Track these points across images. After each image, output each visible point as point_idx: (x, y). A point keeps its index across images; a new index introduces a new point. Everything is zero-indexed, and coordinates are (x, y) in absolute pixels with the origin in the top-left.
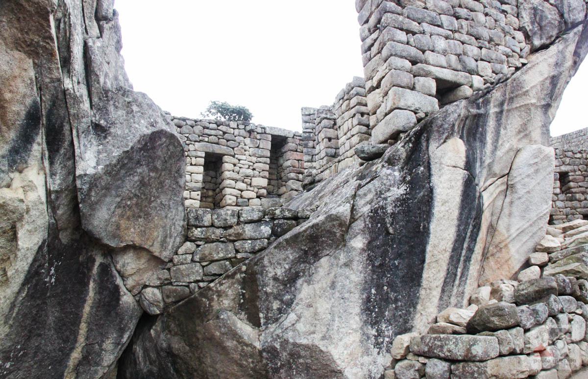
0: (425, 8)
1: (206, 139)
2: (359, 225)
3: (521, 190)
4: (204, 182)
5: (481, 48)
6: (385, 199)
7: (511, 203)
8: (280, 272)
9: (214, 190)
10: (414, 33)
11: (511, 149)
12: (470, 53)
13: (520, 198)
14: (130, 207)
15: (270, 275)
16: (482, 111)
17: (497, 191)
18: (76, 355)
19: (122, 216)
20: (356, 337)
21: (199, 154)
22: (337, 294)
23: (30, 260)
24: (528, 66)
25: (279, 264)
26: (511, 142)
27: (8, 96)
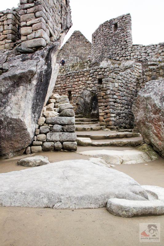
6: (43, 69)
22: (26, 101)
25: (4, 86)
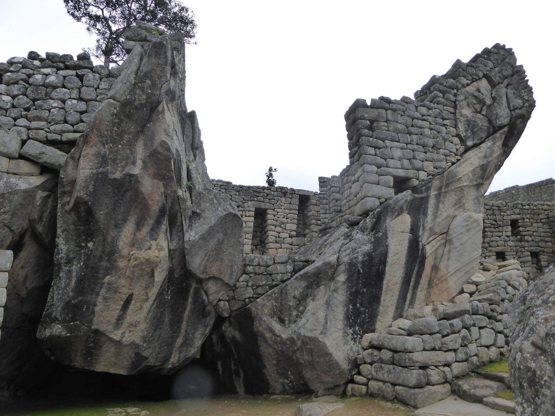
0: (388, 130)
1: (256, 199)
2: (342, 268)
3: (456, 243)
4: (254, 227)
5: (426, 153)
7: (449, 251)
8: (297, 293)
9: (261, 232)
10: (379, 148)
11: (448, 217)
12: (417, 157)
13: (455, 248)
14: (212, 256)
15: (292, 295)
16: (424, 195)
17: (438, 244)
18: (179, 341)
19: (207, 261)
20: (340, 333)
21: (251, 209)
24: (462, 161)
26: (448, 212)
27: (151, 202)
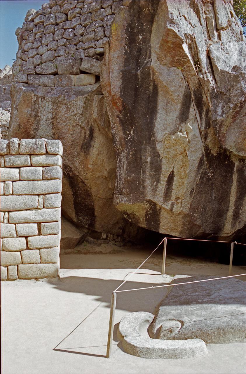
18: (230, 213)
23: (197, 165)
